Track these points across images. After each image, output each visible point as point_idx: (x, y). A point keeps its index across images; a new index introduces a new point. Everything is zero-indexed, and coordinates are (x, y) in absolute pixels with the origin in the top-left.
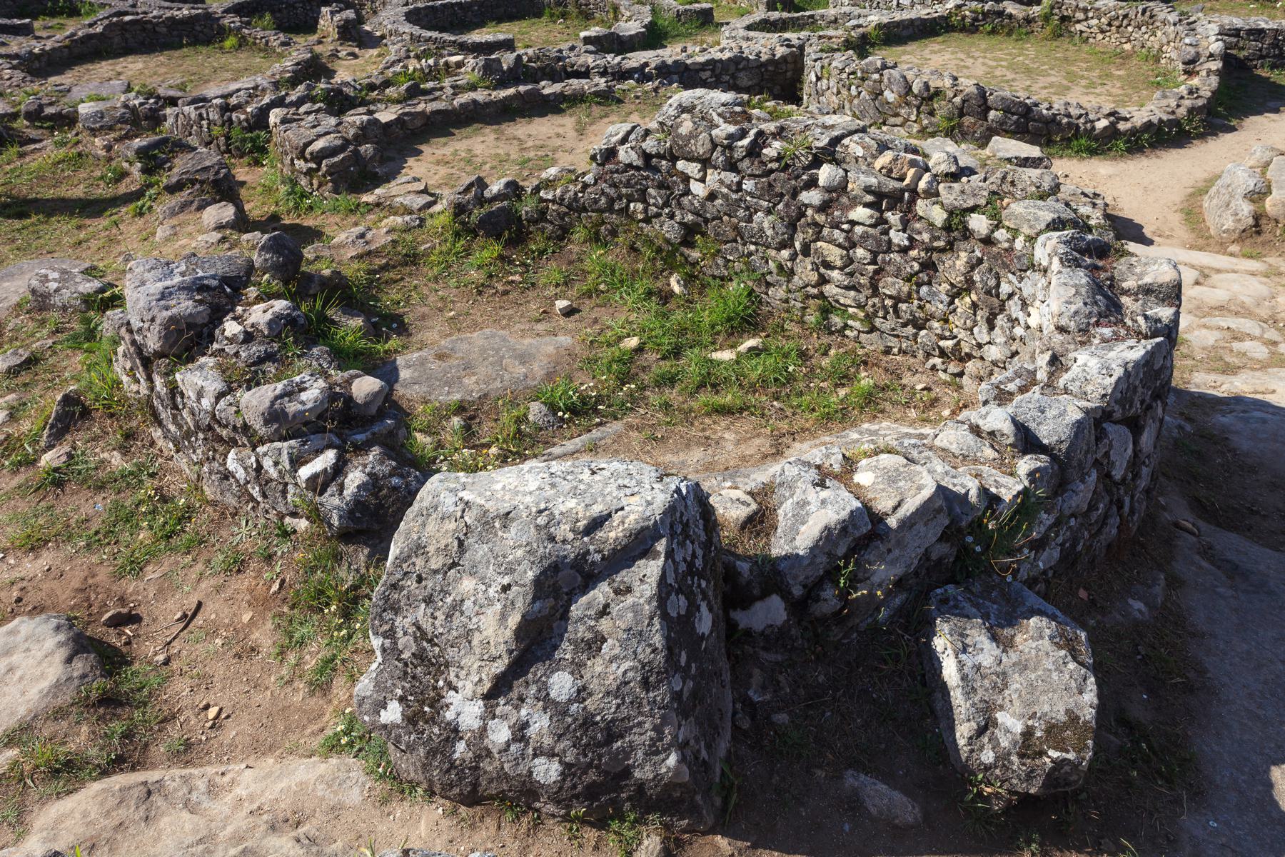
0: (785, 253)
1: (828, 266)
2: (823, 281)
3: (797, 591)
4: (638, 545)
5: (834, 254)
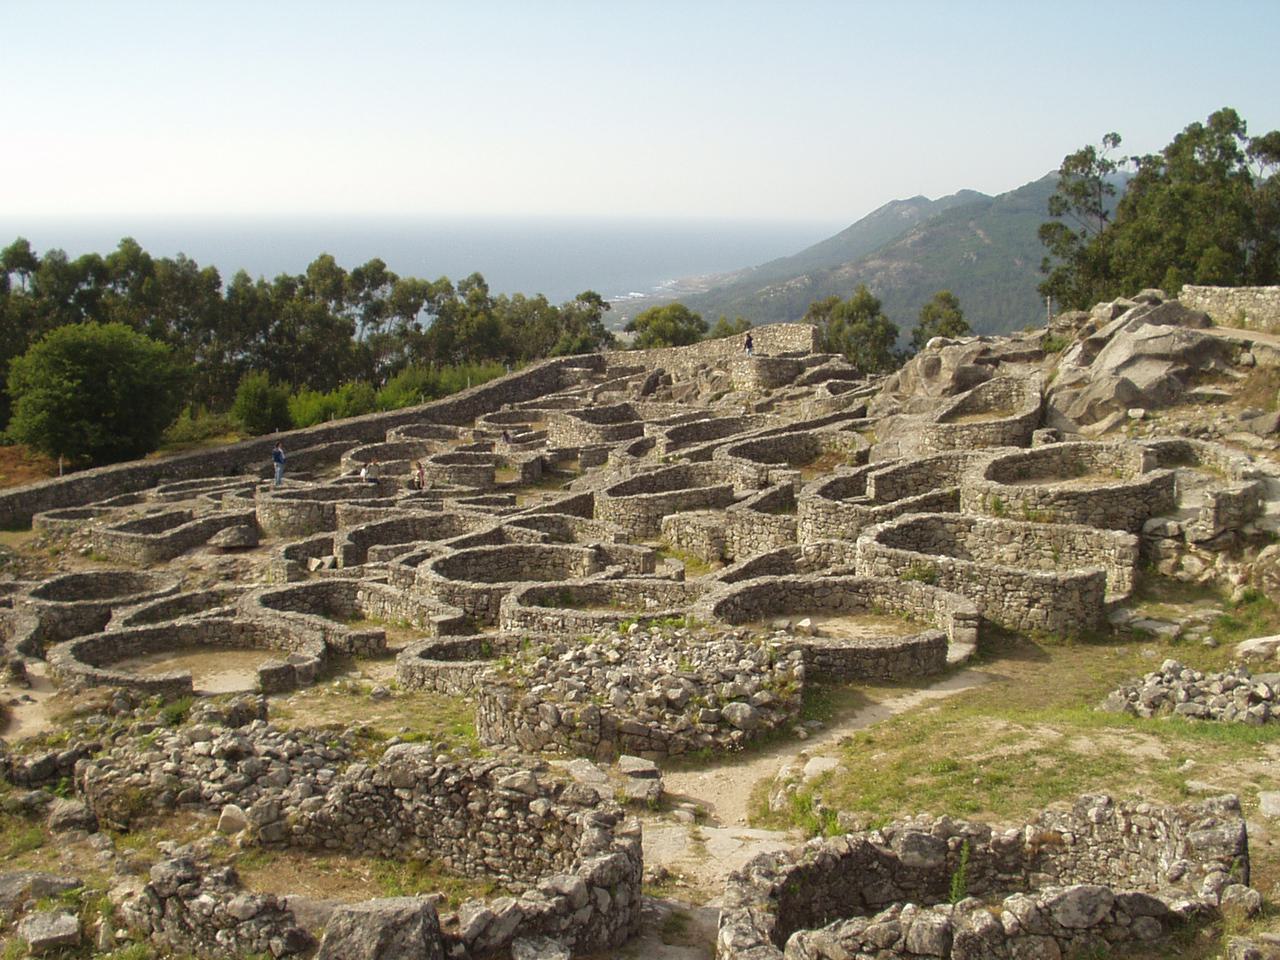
0: (462, 840)
1: (486, 845)
2: (485, 854)
3: (469, 942)
4: (413, 918)
5: (489, 836)
